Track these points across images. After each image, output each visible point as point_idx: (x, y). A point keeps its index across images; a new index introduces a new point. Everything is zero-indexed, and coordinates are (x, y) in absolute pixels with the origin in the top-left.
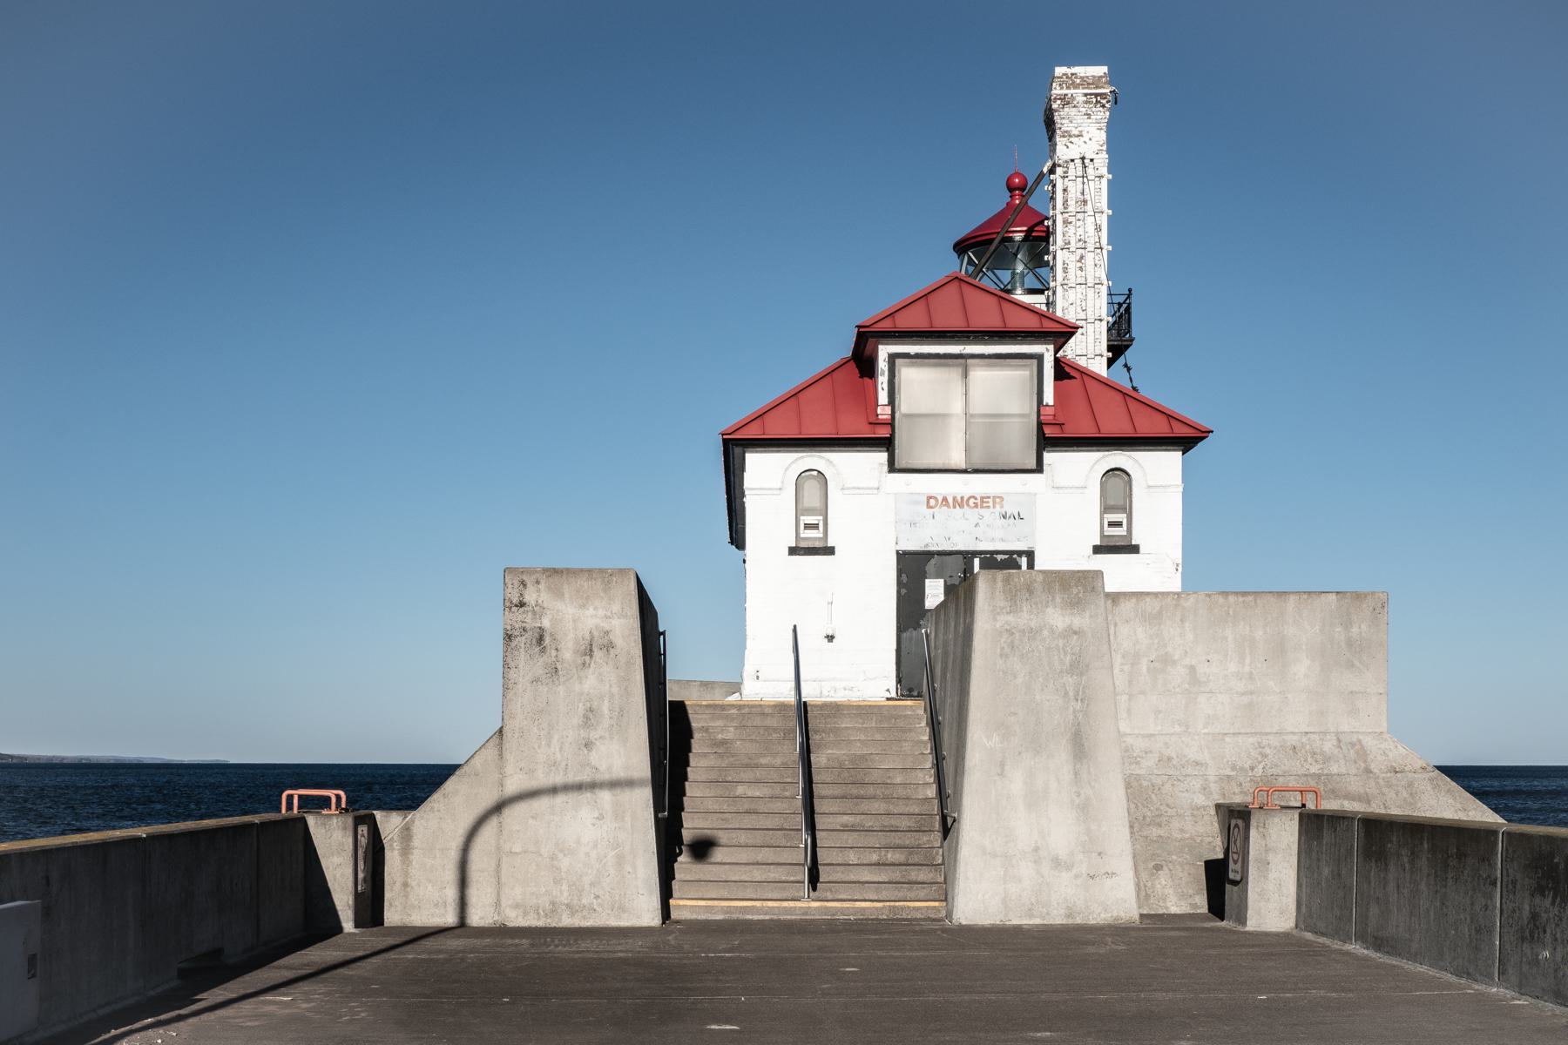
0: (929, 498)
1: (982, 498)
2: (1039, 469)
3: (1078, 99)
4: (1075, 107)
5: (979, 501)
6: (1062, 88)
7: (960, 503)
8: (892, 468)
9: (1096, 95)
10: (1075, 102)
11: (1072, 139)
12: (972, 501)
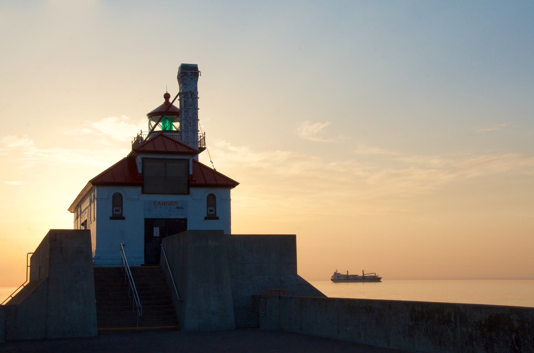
0: (155, 202)
1: (171, 202)
2: (188, 193)
3: (189, 73)
4: (188, 76)
5: (170, 203)
6: (184, 70)
7: (164, 203)
8: (143, 192)
9: (194, 72)
10: (188, 75)
11: (187, 86)
12: (168, 203)
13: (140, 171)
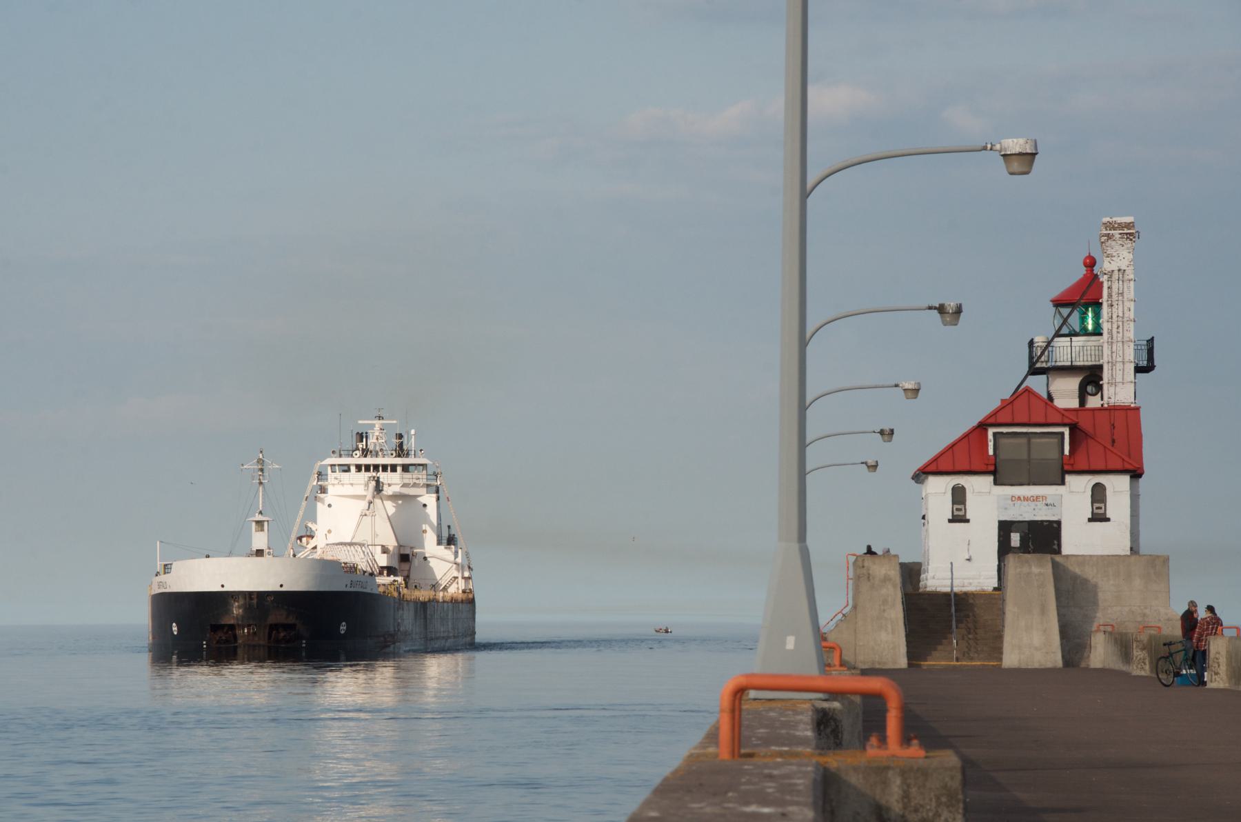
0: (1013, 497)
1: (1037, 497)
2: (1063, 483)
4: (1114, 240)
6: (1106, 230)
7: (1026, 499)
8: (996, 483)
9: (1127, 234)
13: (991, 452)
